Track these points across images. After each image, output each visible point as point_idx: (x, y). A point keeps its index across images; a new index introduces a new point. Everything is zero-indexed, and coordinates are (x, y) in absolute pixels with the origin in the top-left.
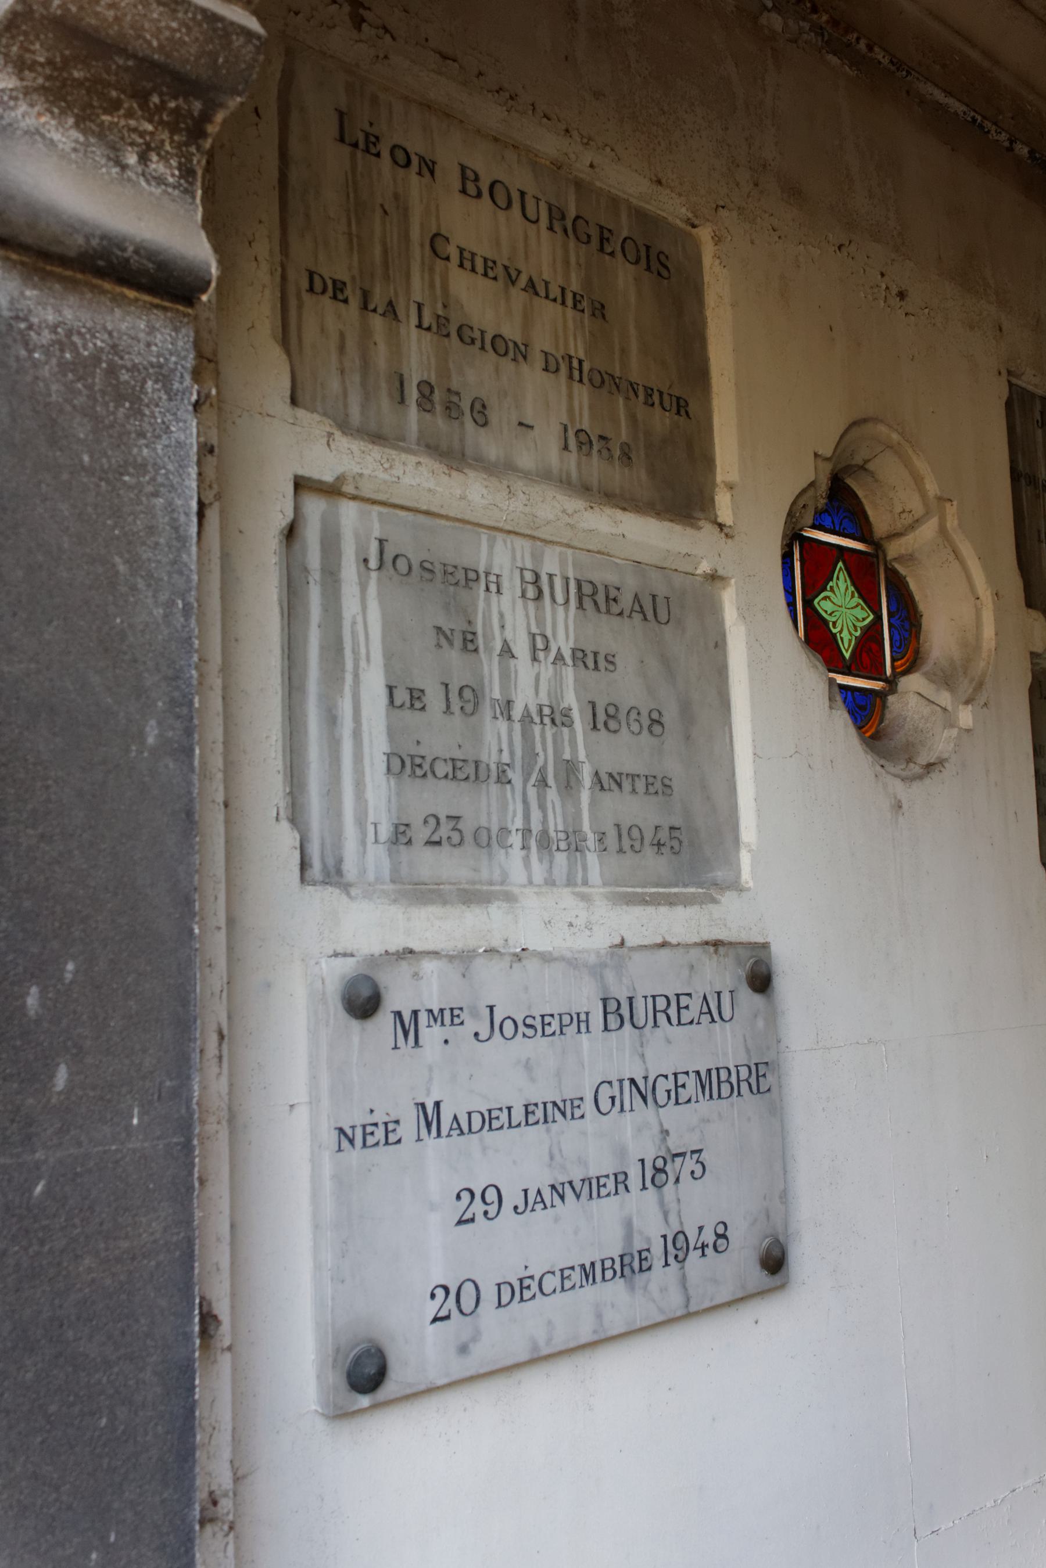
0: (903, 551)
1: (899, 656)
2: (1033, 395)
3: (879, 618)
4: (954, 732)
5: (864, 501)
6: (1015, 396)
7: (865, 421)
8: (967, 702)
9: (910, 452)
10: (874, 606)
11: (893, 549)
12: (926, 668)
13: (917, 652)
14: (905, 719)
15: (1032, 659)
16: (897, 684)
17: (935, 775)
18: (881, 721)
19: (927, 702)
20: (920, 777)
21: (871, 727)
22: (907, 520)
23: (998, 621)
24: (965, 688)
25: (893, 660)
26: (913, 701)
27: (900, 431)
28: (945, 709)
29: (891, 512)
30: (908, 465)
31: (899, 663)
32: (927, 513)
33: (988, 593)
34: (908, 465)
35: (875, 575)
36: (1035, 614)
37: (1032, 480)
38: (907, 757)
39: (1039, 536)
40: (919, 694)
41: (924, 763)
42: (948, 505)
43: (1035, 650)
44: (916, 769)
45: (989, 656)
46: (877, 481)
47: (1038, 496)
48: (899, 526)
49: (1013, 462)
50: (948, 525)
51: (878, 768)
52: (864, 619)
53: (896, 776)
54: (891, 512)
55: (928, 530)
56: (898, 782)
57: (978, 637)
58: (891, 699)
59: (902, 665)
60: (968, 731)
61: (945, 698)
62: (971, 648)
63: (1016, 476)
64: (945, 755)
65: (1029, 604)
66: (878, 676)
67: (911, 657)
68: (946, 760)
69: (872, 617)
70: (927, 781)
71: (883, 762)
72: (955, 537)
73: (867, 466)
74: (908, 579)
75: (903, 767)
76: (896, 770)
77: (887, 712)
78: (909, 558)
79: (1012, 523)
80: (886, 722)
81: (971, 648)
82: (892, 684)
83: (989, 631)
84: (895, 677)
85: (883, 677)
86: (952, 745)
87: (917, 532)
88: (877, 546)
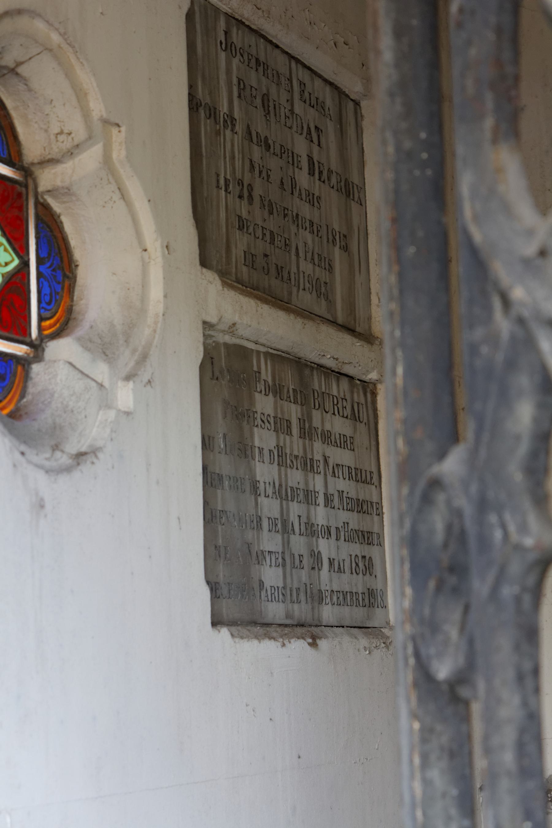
0: (59, 183)
1: (47, 314)
2: (217, 10)
3: (25, 264)
4: (112, 414)
5: (14, 114)
6: (196, 8)
7: (19, 12)
8: (128, 378)
9: (73, 60)
10: (21, 250)
11: (46, 179)
12: (80, 331)
13: (70, 310)
14: (52, 395)
15: (204, 329)
16: (43, 350)
17: (86, 468)
18: (23, 396)
19: (80, 375)
20: (68, 470)
21: (10, 402)
22: (66, 143)
23: (168, 280)
24: (126, 360)
25: (41, 319)
26: (63, 373)
27: (62, 31)
28: (101, 386)
29: (46, 131)
30: (69, 74)
31: (47, 323)
32: (90, 138)
33: (158, 244)
34: (69, 74)
35: (22, 208)
36: (210, 276)
37: (213, 113)
38: (53, 443)
39: (218, 181)
40: (71, 364)
41: (74, 451)
42: (115, 131)
43: (208, 319)
44: (64, 460)
45: (156, 323)
46: (30, 90)
47: (218, 133)
48: (55, 151)
49: (191, 87)
50: (115, 155)
51: (18, 455)
52: (7, 264)
53: (39, 466)
54: (46, 131)
55: (89, 160)
56: (41, 476)
57: (144, 298)
58: (36, 368)
59: (51, 327)
60: (128, 414)
61: (101, 371)
62: (135, 311)
63: (194, 104)
64: (100, 443)
65: (204, 262)
66: (21, 338)
67: (62, 318)
68: (100, 449)
69: (16, 262)
70: (76, 474)
71: (23, 448)
72: (121, 171)
73: (20, 70)
74: (63, 219)
75: (48, 455)
76: (39, 459)
77: (30, 384)
78: (65, 192)
79: (188, 162)
80: (28, 398)
81: (135, 311)
82: (37, 348)
83: (156, 292)
84: (42, 341)
85: (27, 339)
86: (108, 430)
87: (77, 160)
88: (27, 172)
